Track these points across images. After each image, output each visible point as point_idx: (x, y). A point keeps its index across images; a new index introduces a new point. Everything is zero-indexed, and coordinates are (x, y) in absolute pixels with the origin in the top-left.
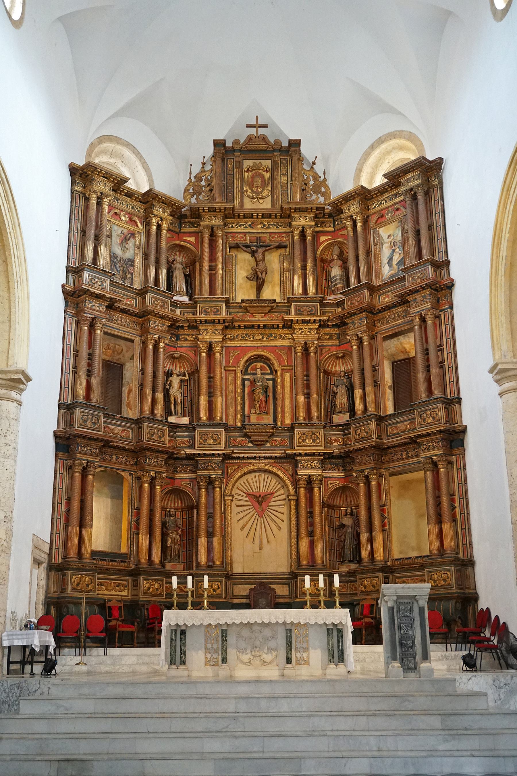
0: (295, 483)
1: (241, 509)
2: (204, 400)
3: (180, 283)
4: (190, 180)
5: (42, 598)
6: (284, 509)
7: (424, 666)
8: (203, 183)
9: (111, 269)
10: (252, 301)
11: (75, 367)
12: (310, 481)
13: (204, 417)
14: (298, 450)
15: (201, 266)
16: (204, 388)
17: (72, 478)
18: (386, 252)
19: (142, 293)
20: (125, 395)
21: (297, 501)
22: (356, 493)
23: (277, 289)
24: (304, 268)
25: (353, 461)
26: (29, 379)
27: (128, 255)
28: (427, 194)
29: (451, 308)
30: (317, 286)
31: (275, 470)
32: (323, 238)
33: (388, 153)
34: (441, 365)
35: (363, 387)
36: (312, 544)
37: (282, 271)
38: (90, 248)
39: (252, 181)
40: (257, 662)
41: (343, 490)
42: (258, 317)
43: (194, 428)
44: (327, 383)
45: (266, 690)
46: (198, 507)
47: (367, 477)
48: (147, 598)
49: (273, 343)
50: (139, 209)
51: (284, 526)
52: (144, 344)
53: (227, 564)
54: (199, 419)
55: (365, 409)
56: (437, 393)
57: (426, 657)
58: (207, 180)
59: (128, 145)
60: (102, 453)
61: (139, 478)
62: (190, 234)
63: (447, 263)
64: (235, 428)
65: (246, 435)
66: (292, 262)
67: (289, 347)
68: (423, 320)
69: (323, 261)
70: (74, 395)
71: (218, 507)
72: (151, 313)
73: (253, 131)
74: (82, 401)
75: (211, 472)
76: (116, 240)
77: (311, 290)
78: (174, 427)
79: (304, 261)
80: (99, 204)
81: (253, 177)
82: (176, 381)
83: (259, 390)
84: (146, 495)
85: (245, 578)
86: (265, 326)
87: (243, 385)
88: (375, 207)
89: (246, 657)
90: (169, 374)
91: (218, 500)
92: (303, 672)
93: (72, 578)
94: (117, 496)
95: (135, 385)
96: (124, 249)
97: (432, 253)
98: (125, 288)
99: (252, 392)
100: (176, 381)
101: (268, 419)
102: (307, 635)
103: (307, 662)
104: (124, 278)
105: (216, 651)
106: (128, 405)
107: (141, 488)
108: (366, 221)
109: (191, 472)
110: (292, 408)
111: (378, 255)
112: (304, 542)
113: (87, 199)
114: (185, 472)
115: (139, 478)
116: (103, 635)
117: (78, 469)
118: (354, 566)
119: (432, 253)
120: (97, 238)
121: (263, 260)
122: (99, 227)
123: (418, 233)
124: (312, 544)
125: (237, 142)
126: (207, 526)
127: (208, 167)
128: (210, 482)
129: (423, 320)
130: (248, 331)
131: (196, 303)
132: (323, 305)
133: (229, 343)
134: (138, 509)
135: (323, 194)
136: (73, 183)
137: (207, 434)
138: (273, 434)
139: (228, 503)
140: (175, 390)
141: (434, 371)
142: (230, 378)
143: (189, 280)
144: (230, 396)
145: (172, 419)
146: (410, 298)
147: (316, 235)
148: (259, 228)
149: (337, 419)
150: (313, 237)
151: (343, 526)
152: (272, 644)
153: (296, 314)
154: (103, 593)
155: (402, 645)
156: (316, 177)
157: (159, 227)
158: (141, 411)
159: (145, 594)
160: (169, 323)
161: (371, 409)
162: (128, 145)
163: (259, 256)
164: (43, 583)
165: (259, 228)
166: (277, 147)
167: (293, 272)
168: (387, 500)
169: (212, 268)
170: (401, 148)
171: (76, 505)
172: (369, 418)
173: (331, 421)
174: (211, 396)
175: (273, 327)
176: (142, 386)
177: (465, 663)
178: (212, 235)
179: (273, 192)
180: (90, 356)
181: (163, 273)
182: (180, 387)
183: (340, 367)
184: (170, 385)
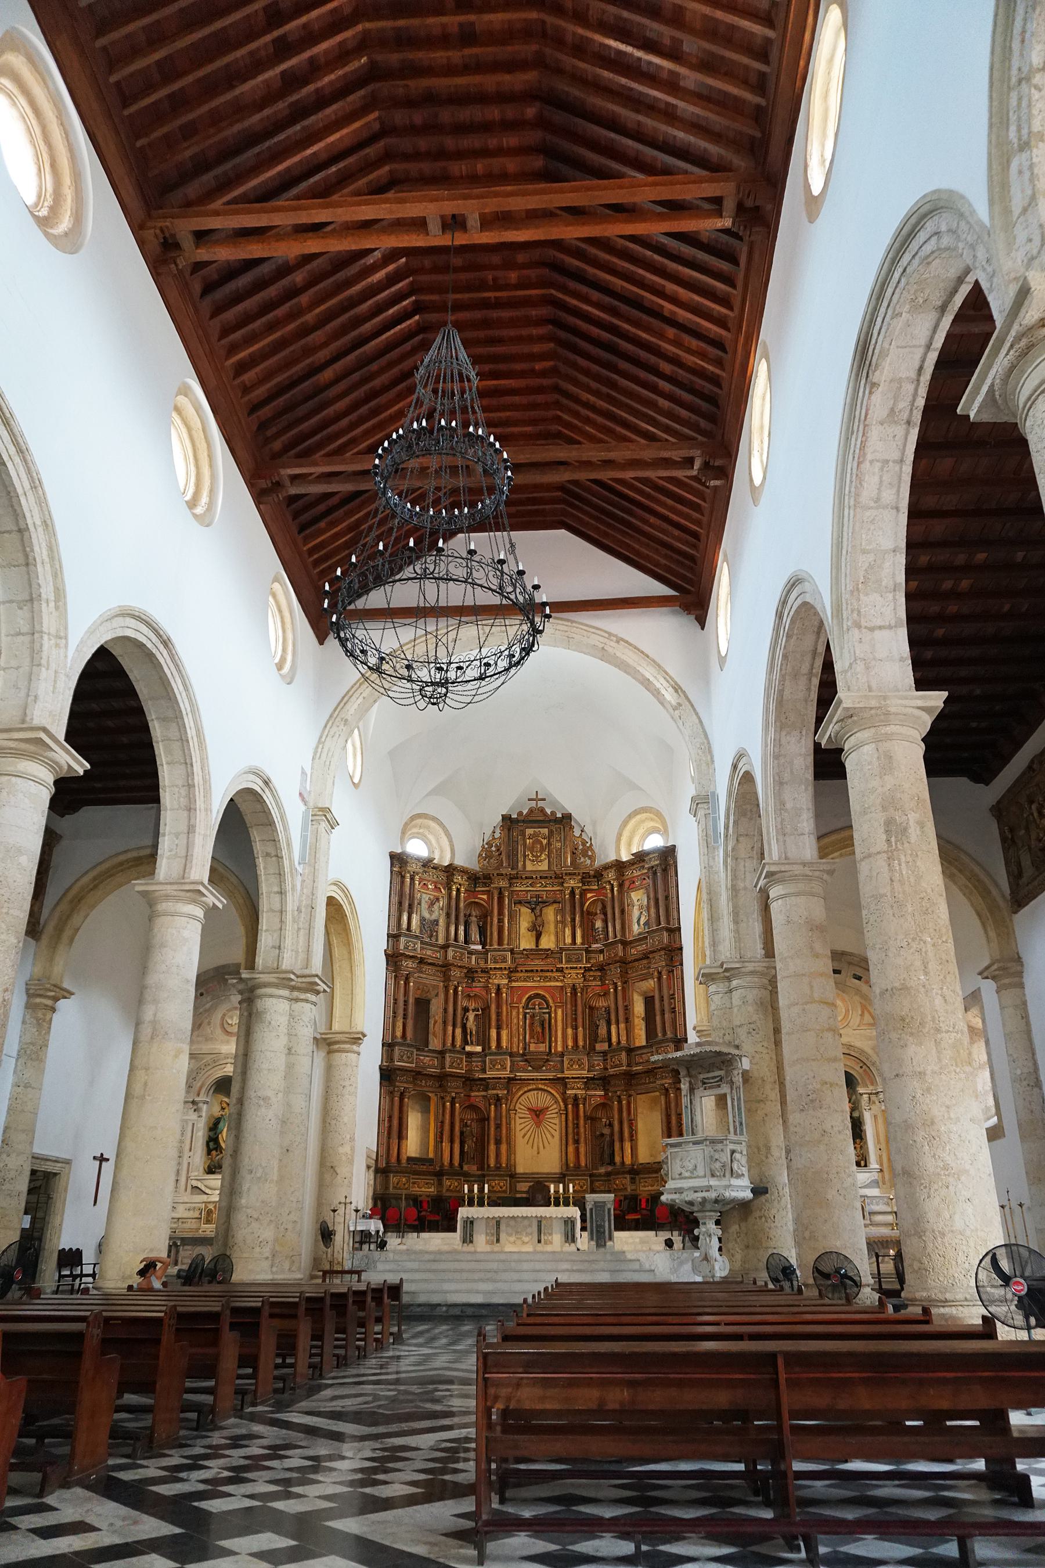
0: (565, 1101)
1: (523, 1120)
2: (494, 1033)
3: (475, 935)
4: (483, 847)
5: (371, 1194)
6: (557, 1121)
7: (609, 1243)
8: (493, 849)
9: (421, 931)
10: (531, 950)
11: (394, 1013)
12: (576, 1098)
13: (494, 1045)
14: (567, 1073)
15: (492, 919)
16: (493, 1023)
17: (392, 1101)
18: (636, 913)
19: (445, 947)
20: (431, 1025)
21: (567, 1114)
22: (612, 1108)
23: (553, 938)
24: (573, 920)
25: (609, 1083)
26: (365, 1036)
27: (434, 917)
29: (682, 965)
30: (583, 937)
31: (549, 1089)
32: (589, 895)
33: (643, 821)
34: (673, 1011)
35: (617, 1023)
38: (405, 917)
39: (533, 847)
40: (519, 1242)
41: (603, 1105)
42: (537, 962)
43: (486, 1056)
44: (591, 1016)
46: (488, 1119)
47: (619, 1097)
48: (448, 1194)
49: (548, 984)
50: (443, 877)
51: (557, 1135)
52: (446, 988)
54: (490, 1048)
55: (619, 1042)
56: (669, 1035)
57: (611, 1238)
58: (496, 846)
60: (415, 1079)
61: (442, 1098)
62: (483, 893)
63: (679, 929)
64: (518, 1054)
65: (526, 1060)
67: (562, 987)
68: (660, 973)
69: (589, 913)
70: (394, 1036)
71: (504, 1120)
72: (452, 965)
73: (533, 804)
74: (400, 1040)
75: (499, 1092)
76: (424, 905)
77: (579, 940)
78: (470, 1054)
79: (573, 914)
80: (412, 879)
81: (533, 843)
82: (471, 1016)
83: (537, 1024)
84: (448, 1111)
85: (526, 1177)
86: (542, 971)
87: (525, 1018)
88: (628, 874)
89: (512, 1239)
90: (466, 1010)
91: (504, 1114)
92: (549, 1248)
93: (393, 1179)
94: (425, 1111)
95: (439, 1018)
96: (431, 912)
97: (668, 922)
98: (431, 945)
99: (532, 1024)
100: (471, 1016)
101: (543, 1048)
102: (551, 1225)
103: (551, 1243)
104: (431, 936)
105: (493, 1235)
106: (434, 1034)
107: (444, 1106)
109: (484, 1090)
110: (563, 1037)
113: (403, 877)
114: (479, 1091)
115: (442, 1098)
116: (416, 1223)
117: (397, 1094)
118: (610, 1168)
119: (668, 922)
120: (411, 906)
121: (541, 915)
122: (412, 897)
125: (520, 813)
126: (496, 1135)
127: (497, 835)
128: (498, 1099)
129: (660, 973)
130: (529, 974)
131: (487, 951)
132: (587, 951)
133: (514, 984)
134: (442, 1122)
135: (590, 858)
136: (392, 865)
137: (496, 1060)
138: (548, 1060)
139: (513, 1116)
140: (471, 1023)
142: (514, 1013)
143: (482, 931)
144: (514, 1028)
145: (468, 1048)
146: (651, 956)
147: (583, 893)
148: (538, 887)
149: (600, 1047)
150: (581, 895)
151: (602, 1135)
152: (529, 1230)
153: (567, 962)
154: (415, 1190)
155: (598, 1231)
156: (584, 843)
157: (458, 890)
159: (448, 1190)
160: (465, 971)
161: (624, 1042)
163: (537, 911)
164: (372, 1182)
165: (538, 887)
166: (553, 818)
168: (636, 1115)
169: (501, 921)
170: (652, 820)
171: (395, 1122)
172: (622, 1049)
173: (594, 1049)
174: (499, 1028)
175: (548, 971)
176: (445, 1023)
177: (666, 1244)
179: (549, 856)
180: (406, 1002)
181: (462, 928)
182: (475, 1020)
183: (602, 1003)
184: (467, 1019)
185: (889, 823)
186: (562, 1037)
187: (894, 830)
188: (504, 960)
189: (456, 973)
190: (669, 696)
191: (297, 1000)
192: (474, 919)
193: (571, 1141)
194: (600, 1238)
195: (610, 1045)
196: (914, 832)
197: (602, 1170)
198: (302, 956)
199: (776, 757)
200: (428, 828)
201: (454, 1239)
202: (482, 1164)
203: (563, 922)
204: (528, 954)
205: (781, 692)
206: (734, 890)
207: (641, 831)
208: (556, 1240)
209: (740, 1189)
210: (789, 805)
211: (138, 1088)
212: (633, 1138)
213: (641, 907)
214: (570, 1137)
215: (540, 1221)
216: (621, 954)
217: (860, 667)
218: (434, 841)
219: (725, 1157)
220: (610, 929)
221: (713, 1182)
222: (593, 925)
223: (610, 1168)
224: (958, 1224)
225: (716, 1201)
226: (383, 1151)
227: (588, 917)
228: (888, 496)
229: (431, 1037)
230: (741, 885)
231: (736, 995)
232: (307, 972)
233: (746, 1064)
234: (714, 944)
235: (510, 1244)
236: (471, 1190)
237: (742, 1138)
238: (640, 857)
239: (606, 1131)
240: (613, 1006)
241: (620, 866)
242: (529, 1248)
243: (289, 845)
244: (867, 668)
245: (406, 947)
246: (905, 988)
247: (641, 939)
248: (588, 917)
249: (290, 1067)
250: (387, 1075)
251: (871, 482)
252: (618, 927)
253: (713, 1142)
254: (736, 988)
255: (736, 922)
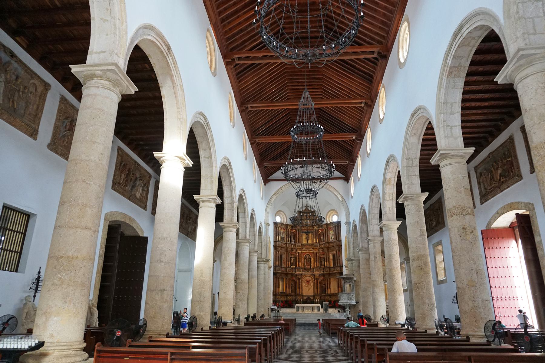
0: (314, 279)
2: (298, 263)
3: (293, 240)
12: (317, 278)
13: (298, 266)
14: (315, 273)
16: (298, 261)
17: (276, 279)
18: (331, 236)
19: (286, 243)
23: (311, 241)
24: (316, 236)
27: (284, 236)
28: (338, 226)
30: (318, 241)
34: (340, 260)
35: (327, 261)
36: (317, 290)
37: (312, 237)
44: (320, 259)
45: (309, 314)
46: (297, 283)
51: (312, 286)
53: (302, 293)
55: (327, 266)
56: (339, 265)
57: (328, 311)
59: (282, 211)
62: (294, 230)
66: (314, 236)
68: (337, 251)
69: (320, 235)
70: (276, 265)
76: (281, 234)
77: (317, 242)
78: (292, 268)
80: (279, 228)
82: (292, 259)
84: (288, 281)
85: (306, 296)
90: (291, 258)
92: (314, 312)
93: (277, 297)
94: (283, 281)
96: (283, 235)
99: (306, 261)
100: (292, 259)
108: (327, 229)
111: (330, 236)
112: (316, 290)
113: (277, 228)
118: (325, 294)
120: (279, 234)
123: (336, 233)
124: (317, 290)
128: (299, 278)
129: (337, 251)
131: (296, 244)
132: (319, 244)
133: (302, 252)
136: (274, 225)
140: (292, 261)
141: (338, 261)
142: (302, 258)
143: (294, 239)
145: (292, 267)
153: (315, 247)
154: (282, 299)
158: (287, 266)
161: (328, 266)
162: (282, 211)
167: (314, 238)
169: (299, 237)
171: (277, 284)
172: (328, 268)
176: (287, 261)
178: (299, 231)
181: (290, 239)
183: (323, 256)
185: (374, 256)
186: (314, 264)
187: (375, 258)
188: (300, 246)
189: (289, 250)
190: (340, 199)
191: (265, 264)
192: (292, 236)
193: (316, 288)
194: (326, 310)
195: (325, 266)
196: (378, 258)
197: (323, 295)
198: (265, 255)
199: (361, 228)
200: (281, 213)
201: (294, 310)
202: (296, 293)
203: (313, 237)
204: (305, 245)
205: (362, 218)
206: (353, 243)
207: (332, 214)
208: (316, 311)
209: (353, 302)
210: (363, 237)
211: (250, 286)
212: (330, 288)
213: (332, 235)
214: (316, 287)
215: (312, 307)
216: (327, 246)
217: (372, 231)
218: (282, 217)
219: (351, 297)
220: (325, 239)
221: (348, 301)
222: (321, 238)
223: (325, 294)
224: (380, 312)
225: (349, 305)
226: (275, 291)
227: (319, 236)
228: (376, 206)
229: (283, 264)
230: (355, 242)
231: (353, 264)
232: (267, 258)
233: (355, 279)
234: (349, 253)
235: (307, 312)
236: (298, 301)
237: (354, 293)
238: (332, 223)
239: (324, 286)
240: (325, 258)
241: (327, 224)
242: (310, 312)
243: (263, 233)
244: (373, 232)
245: (278, 244)
246: (375, 281)
247: (332, 242)
248: (319, 236)
249: (264, 277)
250: (275, 274)
251: (374, 205)
252: (327, 239)
253: (348, 294)
254: (354, 263)
255: (354, 249)
